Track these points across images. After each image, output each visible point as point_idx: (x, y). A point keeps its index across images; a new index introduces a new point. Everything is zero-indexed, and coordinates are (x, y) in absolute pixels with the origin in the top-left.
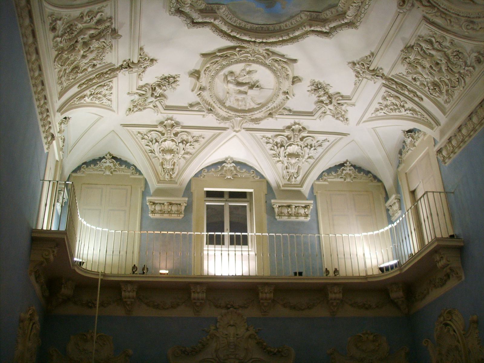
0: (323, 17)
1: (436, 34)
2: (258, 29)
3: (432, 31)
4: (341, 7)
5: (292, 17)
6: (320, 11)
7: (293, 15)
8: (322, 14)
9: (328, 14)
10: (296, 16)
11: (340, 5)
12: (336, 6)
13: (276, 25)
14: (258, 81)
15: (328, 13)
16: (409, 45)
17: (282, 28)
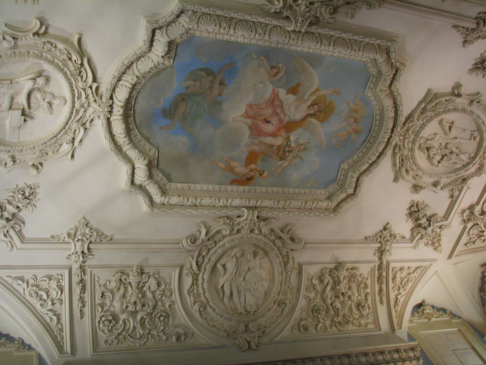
0: (154, 173)
1: (170, 285)
2: (130, 105)
3: (170, 281)
4: (170, 187)
5: (147, 139)
6: (160, 167)
7: (151, 141)
8: (157, 170)
9: (159, 176)
10: (150, 143)
11: (173, 184)
12: (170, 180)
13: (134, 125)
14: (32, 118)
15: (159, 176)
16: (144, 268)
17: (132, 132)
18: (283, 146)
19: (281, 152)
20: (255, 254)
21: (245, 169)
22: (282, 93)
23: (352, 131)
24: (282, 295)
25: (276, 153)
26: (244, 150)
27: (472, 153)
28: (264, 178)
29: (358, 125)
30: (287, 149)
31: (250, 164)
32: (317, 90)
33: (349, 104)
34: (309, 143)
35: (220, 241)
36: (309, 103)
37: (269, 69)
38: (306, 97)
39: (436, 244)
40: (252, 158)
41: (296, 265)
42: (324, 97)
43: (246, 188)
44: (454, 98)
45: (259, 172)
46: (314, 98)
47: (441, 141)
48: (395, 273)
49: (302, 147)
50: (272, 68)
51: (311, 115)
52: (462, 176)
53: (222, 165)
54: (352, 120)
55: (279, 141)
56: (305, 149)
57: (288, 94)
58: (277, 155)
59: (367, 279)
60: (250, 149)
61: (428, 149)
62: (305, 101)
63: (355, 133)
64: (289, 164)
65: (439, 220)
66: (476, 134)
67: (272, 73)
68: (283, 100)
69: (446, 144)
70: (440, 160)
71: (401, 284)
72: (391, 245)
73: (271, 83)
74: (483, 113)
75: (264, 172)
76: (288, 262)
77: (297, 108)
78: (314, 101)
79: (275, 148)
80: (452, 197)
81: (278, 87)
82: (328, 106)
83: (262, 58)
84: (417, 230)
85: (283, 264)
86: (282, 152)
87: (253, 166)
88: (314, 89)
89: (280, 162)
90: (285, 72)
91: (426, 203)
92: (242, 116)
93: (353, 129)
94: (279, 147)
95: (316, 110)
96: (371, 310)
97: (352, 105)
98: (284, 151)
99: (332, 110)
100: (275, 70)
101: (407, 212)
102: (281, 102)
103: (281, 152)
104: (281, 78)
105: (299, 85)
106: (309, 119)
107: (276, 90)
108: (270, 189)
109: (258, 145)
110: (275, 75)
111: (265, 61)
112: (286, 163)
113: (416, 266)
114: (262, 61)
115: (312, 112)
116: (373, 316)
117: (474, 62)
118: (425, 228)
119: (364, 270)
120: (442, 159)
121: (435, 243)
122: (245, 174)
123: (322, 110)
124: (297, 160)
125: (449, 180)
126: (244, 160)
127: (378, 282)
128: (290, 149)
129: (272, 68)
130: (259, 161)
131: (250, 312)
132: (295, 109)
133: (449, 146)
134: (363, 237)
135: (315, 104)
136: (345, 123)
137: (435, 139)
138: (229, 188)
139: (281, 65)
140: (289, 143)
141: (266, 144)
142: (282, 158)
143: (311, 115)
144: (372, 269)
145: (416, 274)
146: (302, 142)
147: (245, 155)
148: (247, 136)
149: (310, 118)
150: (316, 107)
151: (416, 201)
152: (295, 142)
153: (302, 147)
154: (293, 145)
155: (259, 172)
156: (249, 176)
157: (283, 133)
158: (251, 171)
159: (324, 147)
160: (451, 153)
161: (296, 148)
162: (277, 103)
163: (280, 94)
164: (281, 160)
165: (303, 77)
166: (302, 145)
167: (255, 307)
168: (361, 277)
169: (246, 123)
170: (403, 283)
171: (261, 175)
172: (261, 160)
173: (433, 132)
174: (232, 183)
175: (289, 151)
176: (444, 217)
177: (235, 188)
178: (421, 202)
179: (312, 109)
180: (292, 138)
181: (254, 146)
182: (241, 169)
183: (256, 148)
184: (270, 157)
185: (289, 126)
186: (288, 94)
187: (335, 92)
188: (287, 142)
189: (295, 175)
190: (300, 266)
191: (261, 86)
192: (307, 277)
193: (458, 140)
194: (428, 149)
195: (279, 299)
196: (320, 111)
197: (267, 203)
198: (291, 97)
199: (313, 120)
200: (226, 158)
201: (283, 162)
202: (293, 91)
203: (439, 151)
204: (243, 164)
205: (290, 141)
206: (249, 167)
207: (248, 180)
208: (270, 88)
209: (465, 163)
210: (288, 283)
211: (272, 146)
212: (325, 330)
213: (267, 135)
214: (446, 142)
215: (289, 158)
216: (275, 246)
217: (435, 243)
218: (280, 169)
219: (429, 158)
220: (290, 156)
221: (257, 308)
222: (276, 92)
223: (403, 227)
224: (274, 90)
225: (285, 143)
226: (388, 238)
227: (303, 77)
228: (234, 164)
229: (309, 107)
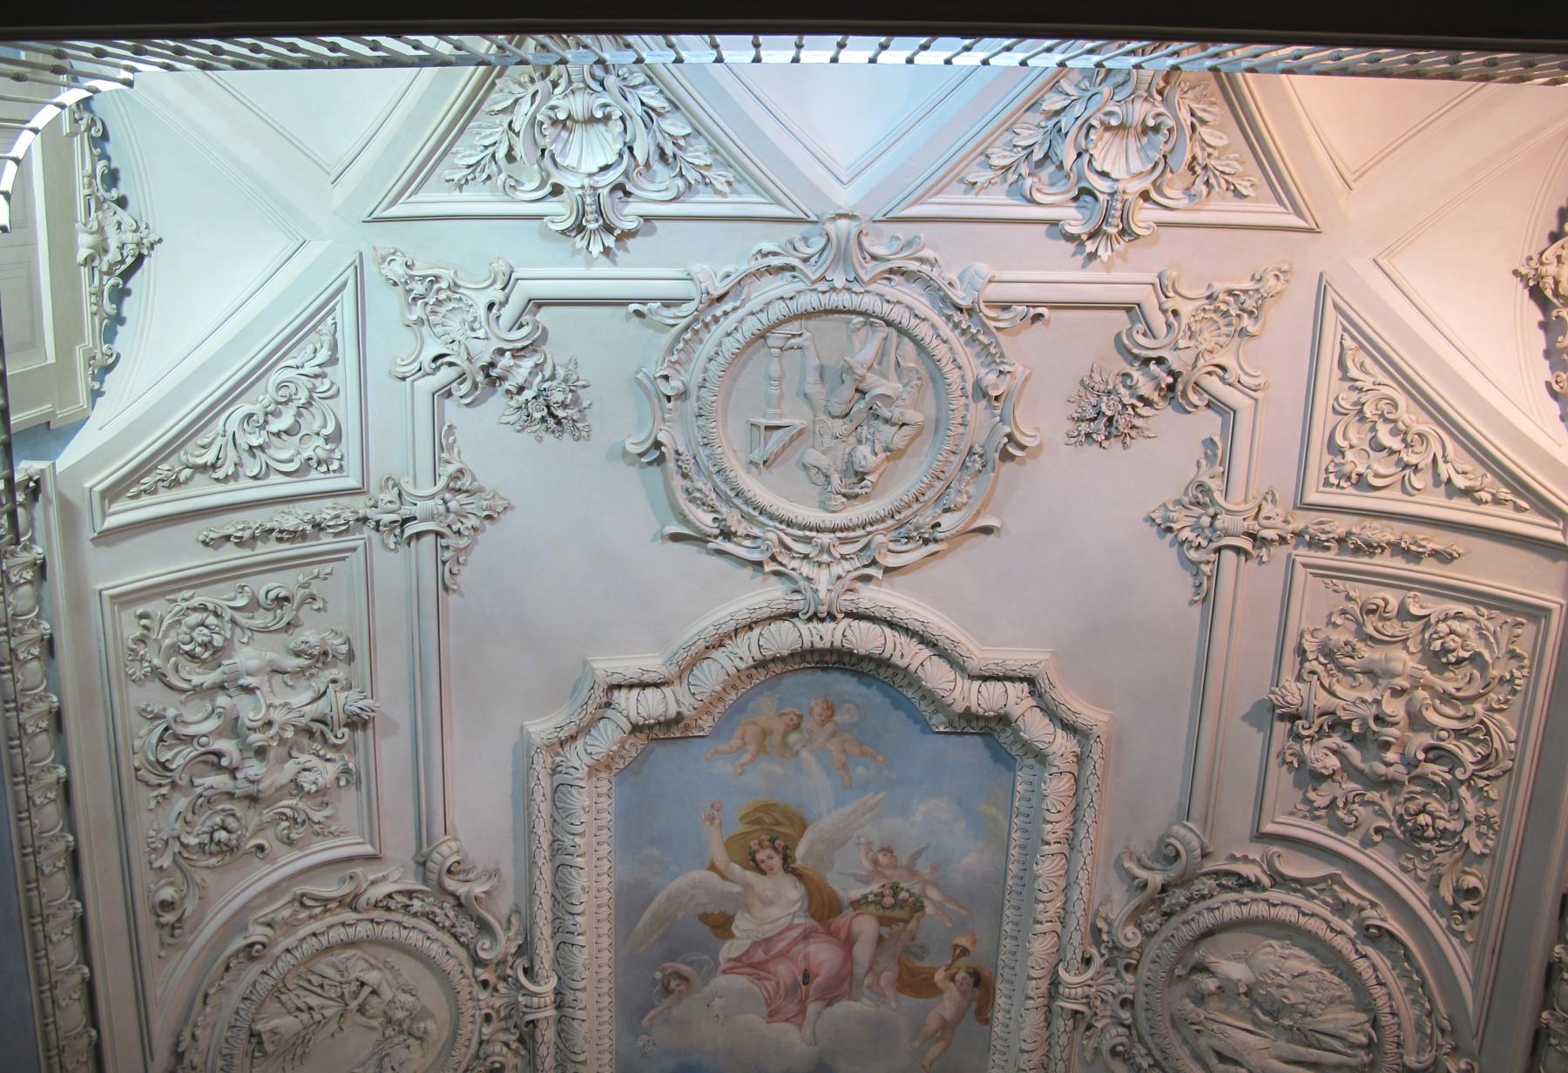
18: (881, 912)
19: (898, 913)
20: (1201, 968)
21: (946, 996)
22: (730, 950)
23: (829, 727)
24: (1344, 917)
25: (901, 925)
26: (894, 1005)
27: (849, 322)
28: (974, 943)
29: (806, 716)
30: (889, 900)
31: (934, 985)
32: (712, 867)
33: (742, 765)
34: (870, 843)
35: (1150, 1054)
36: (750, 876)
37: (672, 997)
38: (736, 888)
39: (1250, 304)
40: (916, 983)
41: (1255, 852)
42: (728, 844)
43: (1001, 987)
44: (671, 464)
45: (955, 959)
46: (736, 868)
47: (828, 441)
48: (1349, 478)
49: (882, 859)
50: (667, 991)
51: (787, 860)
52: (949, 318)
53: (935, 1050)
54: (794, 738)
55: (866, 926)
56: (887, 850)
57: (731, 936)
58: (907, 922)
59: (1349, 598)
60: (890, 992)
61: (861, 476)
62: (747, 886)
63: (833, 714)
64: (935, 885)
65: (1141, 327)
66: (775, 339)
67: (683, 987)
68: (749, 942)
69: (834, 417)
70: (894, 424)
71: (1392, 452)
72: (1229, 512)
73: (706, 984)
74: (701, 342)
75: (956, 946)
76: (1240, 876)
77: (767, 903)
78: (745, 867)
79: (885, 931)
80: (1039, 316)
81: (717, 963)
82: (753, 822)
83: (645, 1022)
84: (1184, 394)
85: (1248, 894)
86: (897, 909)
87: (939, 977)
88: (714, 878)
89: (929, 909)
90: (674, 960)
91: (1073, 389)
92: (800, 1027)
93: (823, 723)
94: (883, 921)
95: (770, 852)
96: (1467, 610)
97: (746, 757)
98: (893, 906)
99: (767, 808)
100: (673, 984)
101: (1115, 444)
102: (755, 945)
103: (898, 913)
104: (690, 964)
105: (705, 918)
106: (799, 863)
107: (723, 965)
108: (1008, 928)
109: (879, 976)
110: (686, 979)
111: (653, 1013)
112: (933, 893)
113: (1337, 373)
114: (654, 1017)
115: (777, 861)
116: (1495, 613)
117: (548, 438)
118: (1175, 375)
119: (1313, 606)
120: (887, 421)
121: (1238, 311)
122: (963, 992)
123: (772, 837)
124: (923, 866)
125: (966, 354)
126: (921, 1000)
127: (1372, 555)
128: (887, 891)
129: (667, 991)
130: (926, 964)
131: (1371, 1038)
132: (777, 904)
133: (839, 409)
134: (1197, 608)
135: (754, 860)
136: (804, 754)
137: (823, 461)
138: (998, 1029)
139: (658, 975)
140: (871, 898)
141: (875, 956)
142: (917, 907)
143: (787, 860)
144: (1315, 575)
145: (1371, 376)
146: (866, 864)
147: (907, 1001)
148: (855, 1006)
149: (794, 861)
150: (760, 856)
151: (1071, 426)
152: (868, 883)
153: (882, 859)
154: (875, 887)
155: (955, 959)
156: (970, 980)
157: (840, 921)
158: (952, 979)
159: (881, 795)
160: (862, 392)
161: (885, 877)
162: (759, 955)
163: (735, 954)
164: (922, 908)
165: (680, 915)
166: (875, 862)
167: (1362, 1017)
168: (1339, 621)
169: (819, 1014)
170: (1396, 444)
171: (965, 952)
172: (921, 958)
173: (803, 473)
174: (987, 1022)
175: (895, 895)
176: (1128, 310)
177: (999, 1016)
178: (1073, 410)
179: (769, 862)
180: (856, 894)
181: (883, 982)
182: (949, 1003)
183: (888, 976)
184: (913, 938)
185: (824, 908)
186: (731, 936)
187: (712, 819)
188: (868, 903)
189: (969, 859)
190: (1261, 837)
191: (717, 1003)
192: (1305, 817)
193: (813, 388)
194: (861, 476)
195: (1353, 933)
196: (772, 841)
197: (1041, 947)
198: (741, 924)
199: (800, 851)
200: (917, 1044)
201: (926, 903)
202: (721, 925)
203: (864, 431)
204: (932, 1000)
205: (865, 897)
206: (940, 985)
207: (981, 984)
208: (720, 980)
209: (894, 333)
210: (1311, 889)
211: (880, 939)
212: (1490, 827)
213: (849, 958)
214: (830, 421)
215: (916, 889)
216: (1184, 907)
217: (1238, 311)
218: (951, 906)
219: (893, 454)
220: (911, 886)
221: (1365, 1011)
222: (731, 964)
223: (1170, 446)
224: (724, 972)
225: (872, 908)
226: (1206, 521)
227: (680, 915)
228: (932, 1022)
229: (763, 872)
